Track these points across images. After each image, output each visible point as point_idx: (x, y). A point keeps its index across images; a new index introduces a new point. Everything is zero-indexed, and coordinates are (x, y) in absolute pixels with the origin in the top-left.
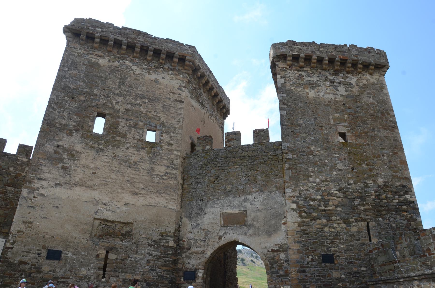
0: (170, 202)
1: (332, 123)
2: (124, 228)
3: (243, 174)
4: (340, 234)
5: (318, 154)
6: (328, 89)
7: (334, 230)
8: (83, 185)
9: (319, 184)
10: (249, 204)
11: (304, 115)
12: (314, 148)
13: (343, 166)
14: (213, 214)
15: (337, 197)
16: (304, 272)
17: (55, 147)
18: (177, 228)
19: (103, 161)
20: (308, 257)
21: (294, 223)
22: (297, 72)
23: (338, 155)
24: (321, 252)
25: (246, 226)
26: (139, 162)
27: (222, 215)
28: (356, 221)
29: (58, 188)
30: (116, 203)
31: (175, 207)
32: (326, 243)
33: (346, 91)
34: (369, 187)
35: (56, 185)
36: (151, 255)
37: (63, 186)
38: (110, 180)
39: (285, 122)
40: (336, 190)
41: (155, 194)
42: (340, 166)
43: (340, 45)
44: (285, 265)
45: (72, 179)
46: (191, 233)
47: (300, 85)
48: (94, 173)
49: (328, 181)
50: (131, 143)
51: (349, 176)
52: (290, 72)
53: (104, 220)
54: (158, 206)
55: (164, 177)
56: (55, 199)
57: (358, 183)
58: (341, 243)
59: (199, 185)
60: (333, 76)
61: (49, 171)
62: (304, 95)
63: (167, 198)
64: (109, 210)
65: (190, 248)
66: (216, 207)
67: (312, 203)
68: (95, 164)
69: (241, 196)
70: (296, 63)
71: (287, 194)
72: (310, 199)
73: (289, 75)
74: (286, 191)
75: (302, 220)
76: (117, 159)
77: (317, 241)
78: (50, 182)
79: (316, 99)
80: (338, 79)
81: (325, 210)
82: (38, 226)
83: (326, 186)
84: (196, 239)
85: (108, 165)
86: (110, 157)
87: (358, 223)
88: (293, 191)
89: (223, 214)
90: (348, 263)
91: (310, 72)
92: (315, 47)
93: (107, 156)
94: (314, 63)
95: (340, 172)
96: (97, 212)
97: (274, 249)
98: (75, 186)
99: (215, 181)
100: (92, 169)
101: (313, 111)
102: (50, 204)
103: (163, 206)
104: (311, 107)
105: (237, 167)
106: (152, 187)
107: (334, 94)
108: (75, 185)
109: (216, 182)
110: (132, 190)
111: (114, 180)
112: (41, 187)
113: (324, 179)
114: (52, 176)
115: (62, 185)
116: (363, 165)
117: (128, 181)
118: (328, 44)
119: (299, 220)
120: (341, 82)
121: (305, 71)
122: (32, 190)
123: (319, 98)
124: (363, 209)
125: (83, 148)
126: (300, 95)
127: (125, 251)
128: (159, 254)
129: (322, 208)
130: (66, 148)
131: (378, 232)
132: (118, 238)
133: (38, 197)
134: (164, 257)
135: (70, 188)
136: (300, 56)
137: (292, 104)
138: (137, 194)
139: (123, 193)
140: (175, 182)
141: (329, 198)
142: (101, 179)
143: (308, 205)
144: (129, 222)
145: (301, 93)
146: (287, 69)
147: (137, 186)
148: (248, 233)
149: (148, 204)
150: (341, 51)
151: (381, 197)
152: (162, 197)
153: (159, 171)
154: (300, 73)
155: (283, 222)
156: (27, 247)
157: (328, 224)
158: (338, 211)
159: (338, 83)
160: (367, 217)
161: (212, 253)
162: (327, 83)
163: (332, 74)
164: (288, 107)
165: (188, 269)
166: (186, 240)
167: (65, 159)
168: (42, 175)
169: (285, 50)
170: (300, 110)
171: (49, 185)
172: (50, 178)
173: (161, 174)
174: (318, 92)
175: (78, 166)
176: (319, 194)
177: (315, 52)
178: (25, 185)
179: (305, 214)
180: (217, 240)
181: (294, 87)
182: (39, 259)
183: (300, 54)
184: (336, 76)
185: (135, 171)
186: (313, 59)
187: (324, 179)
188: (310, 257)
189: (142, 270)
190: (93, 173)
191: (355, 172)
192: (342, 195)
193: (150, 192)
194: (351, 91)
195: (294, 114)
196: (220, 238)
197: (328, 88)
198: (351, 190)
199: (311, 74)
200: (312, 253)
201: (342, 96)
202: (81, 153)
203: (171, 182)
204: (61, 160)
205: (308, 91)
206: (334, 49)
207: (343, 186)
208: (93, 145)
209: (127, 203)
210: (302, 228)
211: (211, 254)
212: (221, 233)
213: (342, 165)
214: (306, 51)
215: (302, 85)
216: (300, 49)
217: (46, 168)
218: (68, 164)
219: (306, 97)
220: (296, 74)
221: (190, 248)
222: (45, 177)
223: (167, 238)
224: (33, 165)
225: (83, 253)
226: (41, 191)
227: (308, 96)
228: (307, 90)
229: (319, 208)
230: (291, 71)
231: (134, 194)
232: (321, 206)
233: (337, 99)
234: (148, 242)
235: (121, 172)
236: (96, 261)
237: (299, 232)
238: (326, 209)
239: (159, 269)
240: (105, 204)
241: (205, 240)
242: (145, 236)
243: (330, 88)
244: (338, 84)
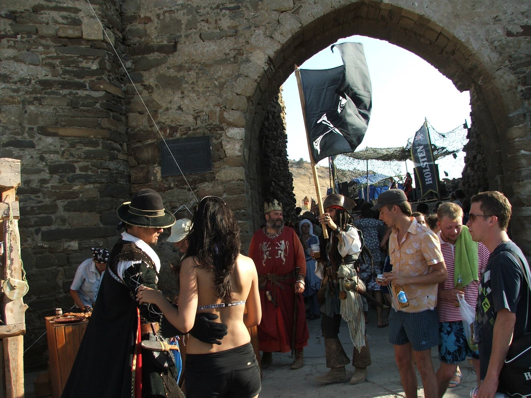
65: (173, 48)
84: (198, 7)
128: (43, 73)
134: (64, 85)
165: (174, 129)
221: (176, 43)
239: (50, 140)
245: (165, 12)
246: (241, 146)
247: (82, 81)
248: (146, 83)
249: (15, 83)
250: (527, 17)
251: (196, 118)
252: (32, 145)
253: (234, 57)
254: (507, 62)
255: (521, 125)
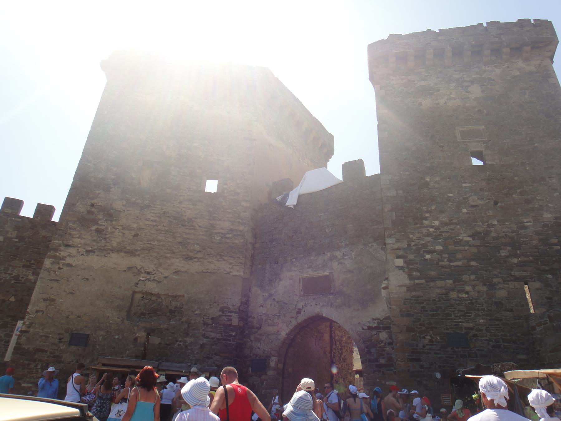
0: (235, 267)
1: (458, 140)
2: (173, 303)
3: (329, 223)
4: (476, 302)
5: (437, 185)
7: (467, 296)
8: (121, 251)
9: (439, 229)
10: (336, 263)
12: (430, 179)
13: (478, 199)
14: (290, 279)
15: (470, 246)
16: (418, 360)
17: (88, 207)
18: (244, 300)
19: (148, 220)
20: (424, 338)
21: (400, 286)
23: (469, 185)
24: (445, 329)
25: (332, 294)
26: (195, 218)
27: (301, 281)
28: (504, 281)
29: (89, 256)
30: (162, 271)
31: (242, 274)
32: (453, 316)
34: (526, 228)
35: (88, 252)
36: (207, 337)
37: (96, 253)
38: (156, 243)
40: (469, 236)
41: (214, 257)
42: (473, 200)
44: (388, 349)
45: (108, 244)
46: (263, 306)
48: (136, 235)
49: (455, 224)
50: (184, 195)
51: (490, 213)
53: (147, 293)
54: (218, 272)
55: (228, 236)
56: (85, 269)
57: (507, 223)
58: (480, 316)
59: (274, 243)
61: (80, 236)
63: (231, 261)
64: (154, 280)
65: (260, 328)
66: (294, 270)
67: (428, 256)
68: (138, 223)
69: (326, 253)
71: (388, 246)
72: (424, 252)
74: (387, 242)
75: (412, 282)
76: (166, 216)
77: (438, 312)
78: (79, 249)
81: (450, 267)
82: (62, 304)
83: (451, 231)
85: (155, 224)
86: (157, 215)
87: (508, 284)
88: (398, 241)
89: (304, 279)
90: (493, 347)
93: (154, 213)
95: (474, 209)
96: (138, 284)
97: (371, 325)
98: (111, 252)
99: (293, 236)
100: (134, 230)
102: (79, 275)
103: (225, 272)
105: (321, 214)
106: (211, 249)
108: (111, 250)
109: (294, 237)
110: (184, 253)
111: (162, 243)
112: (69, 255)
113: (448, 221)
114: (83, 241)
115: (94, 252)
116: (514, 196)
117: (180, 243)
119: (407, 282)
122: (57, 259)
124: (516, 262)
125: (123, 205)
127: (172, 333)
128: (218, 336)
129: (446, 263)
130: (101, 206)
131: (547, 298)
132: (165, 315)
133: (65, 268)
134: (224, 340)
135: (105, 255)
138: (191, 258)
139: (173, 258)
140: (242, 241)
141: (457, 248)
142: (145, 242)
143: (422, 259)
144: (179, 294)
147: (192, 249)
148: (335, 304)
149: (204, 271)
151: (549, 242)
152: (224, 260)
153: (222, 229)
155: (383, 286)
156: (46, 330)
157: (455, 287)
158: (472, 266)
160: (525, 274)
161: (287, 332)
165: (257, 356)
166: (255, 316)
167: (100, 220)
168: (71, 241)
171: (79, 252)
172: (81, 244)
173: (223, 231)
175: (116, 227)
176: (439, 243)
178: (49, 253)
179: (418, 274)
180: (294, 315)
182: (61, 344)
185: (190, 229)
187: (448, 221)
188: (428, 337)
189: (194, 358)
190: (135, 236)
191: (501, 207)
192: (478, 242)
193: (209, 254)
196: (299, 312)
198: (493, 234)
199: (426, 76)
200: (431, 332)
202: (120, 211)
203: (237, 241)
204: (95, 222)
207: (479, 229)
208: (137, 202)
209: (177, 270)
210: (414, 293)
211: (287, 334)
212: (300, 305)
213: (477, 199)
217: (76, 233)
218: (104, 225)
221: (261, 326)
222: (74, 243)
223: (229, 314)
224: (60, 230)
225: (117, 337)
226: (69, 260)
229: (440, 263)
231: (187, 258)
232: (443, 261)
234: (203, 321)
235: (171, 232)
236: (132, 346)
237: (408, 299)
238: (451, 264)
239: (217, 357)
240: (148, 273)
241: (280, 316)
242: (200, 313)
245: (259, 316)
246: (275, 364)
247: (230, 338)
248: (251, 339)
249: (210, 339)
250: (370, 323)
251: (263, 353)
252: (212, 358)
253: (277, 332)
254: (362, 340)
255: (365, 364)
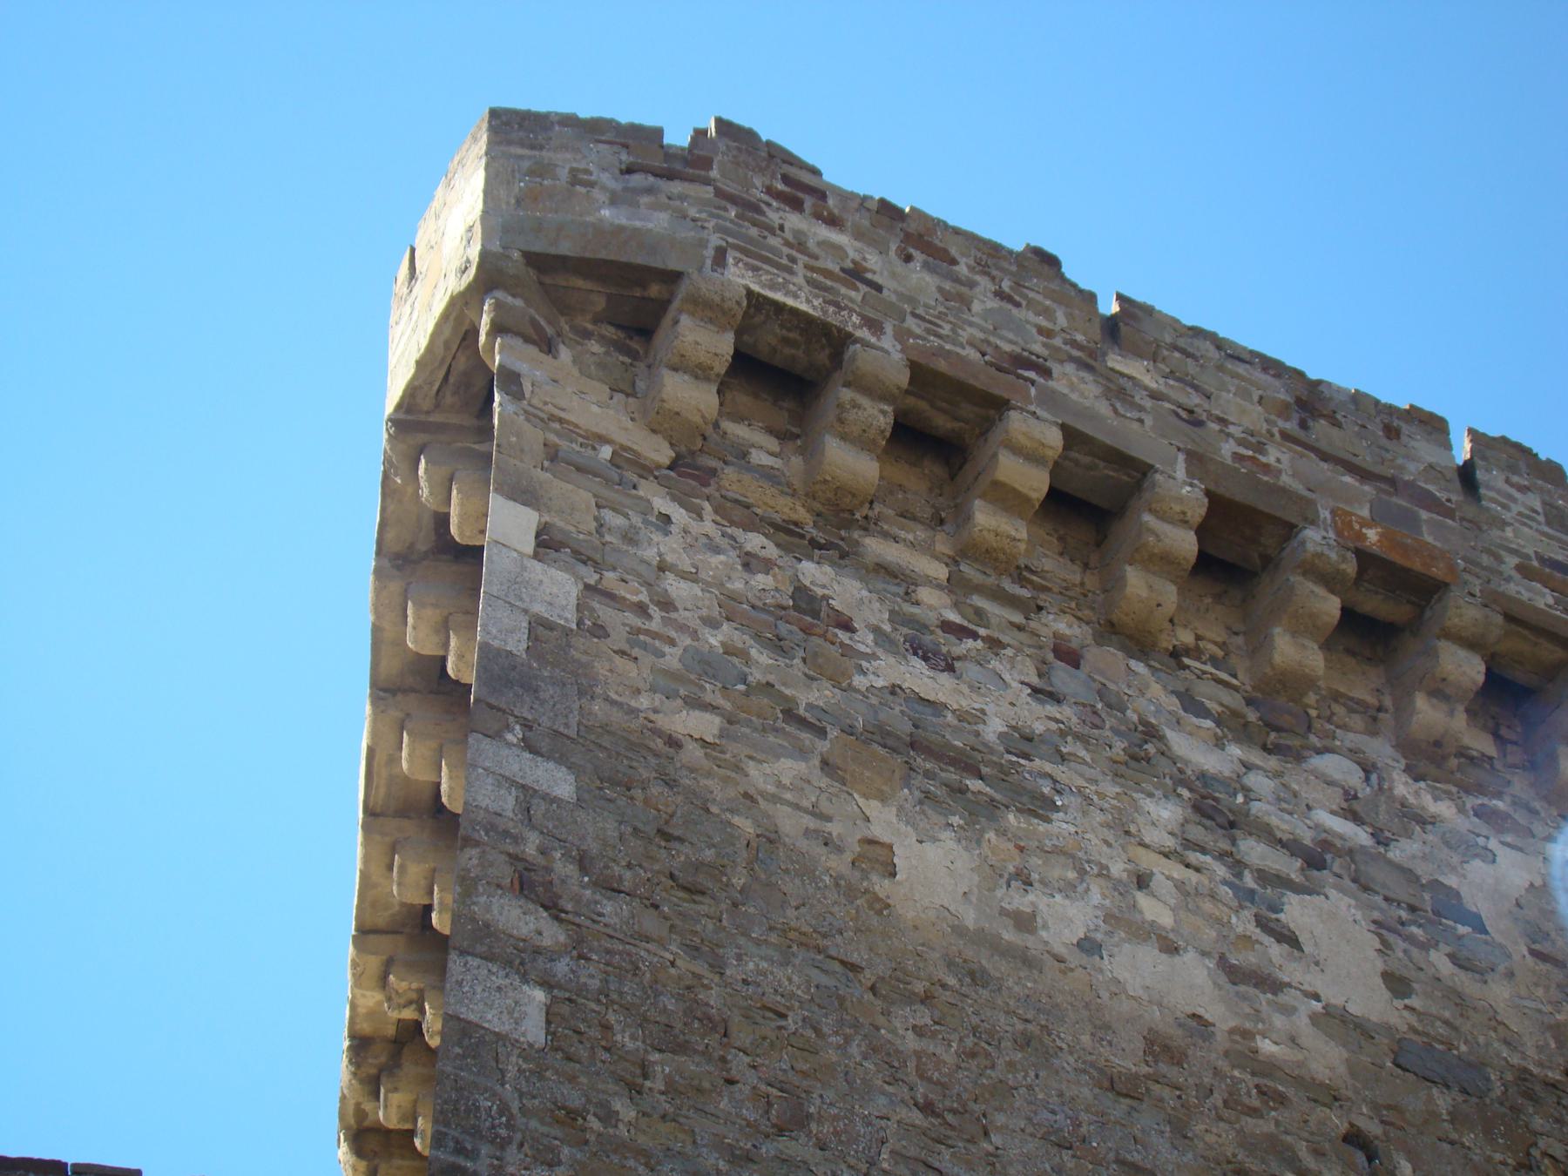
6: (1159, 882)
11: (795, 1122)
22: (772, 551)
33: (1397, 984)
39: (504, 1144)
43: (1358, 398)
47: (802, 722)
52: (679, 514)
60: (1235, 751)
62: (839, 864)
70: (772, 444)
73: (670, 547)
79: (996, 966)
80: (1289, 800)
91: (935, 604)
92: (1047, 313)
94: (1006, 498)
101: (927, 1108)
104: (911, 1042)
107: (1235, 974)
118: (1219, 343)
120: (1326, 845)
121: (885, 571)
123: (1027, 961)
126: (771, 839)
136: (837, 357)
137: (650, 923)
145: (790, 824)
146: (646, 470)
150: (1366, 459)
154: (813, 573)
159: (1291, 847)
162: (1148, 805)
163: (1218, 723)
164: (579, 948)
169: (658, 222)
170: (743, 1035)
174: (1024, 880)
177: (1047, 373)
181: (706, 725)
183: (851, 321)
184: (1273, 762)
186: (1017, 450)
194: (1459, 1000)
195: (663, 1066)
197: (1165, 872)
199: (947, 626)
201: (1335, 1020)
205: (883, 821)
206: (1284, 411)
214: (933, 330)
215: (821, 733)
216: (856, 274)
219: (851, 893)
220: (750, 562)
227: (881, 886)
228: (873, 807)
230: (699, 514)
233: (1266, 1046)
243: (1178, 872)
244: (1292, 867)
